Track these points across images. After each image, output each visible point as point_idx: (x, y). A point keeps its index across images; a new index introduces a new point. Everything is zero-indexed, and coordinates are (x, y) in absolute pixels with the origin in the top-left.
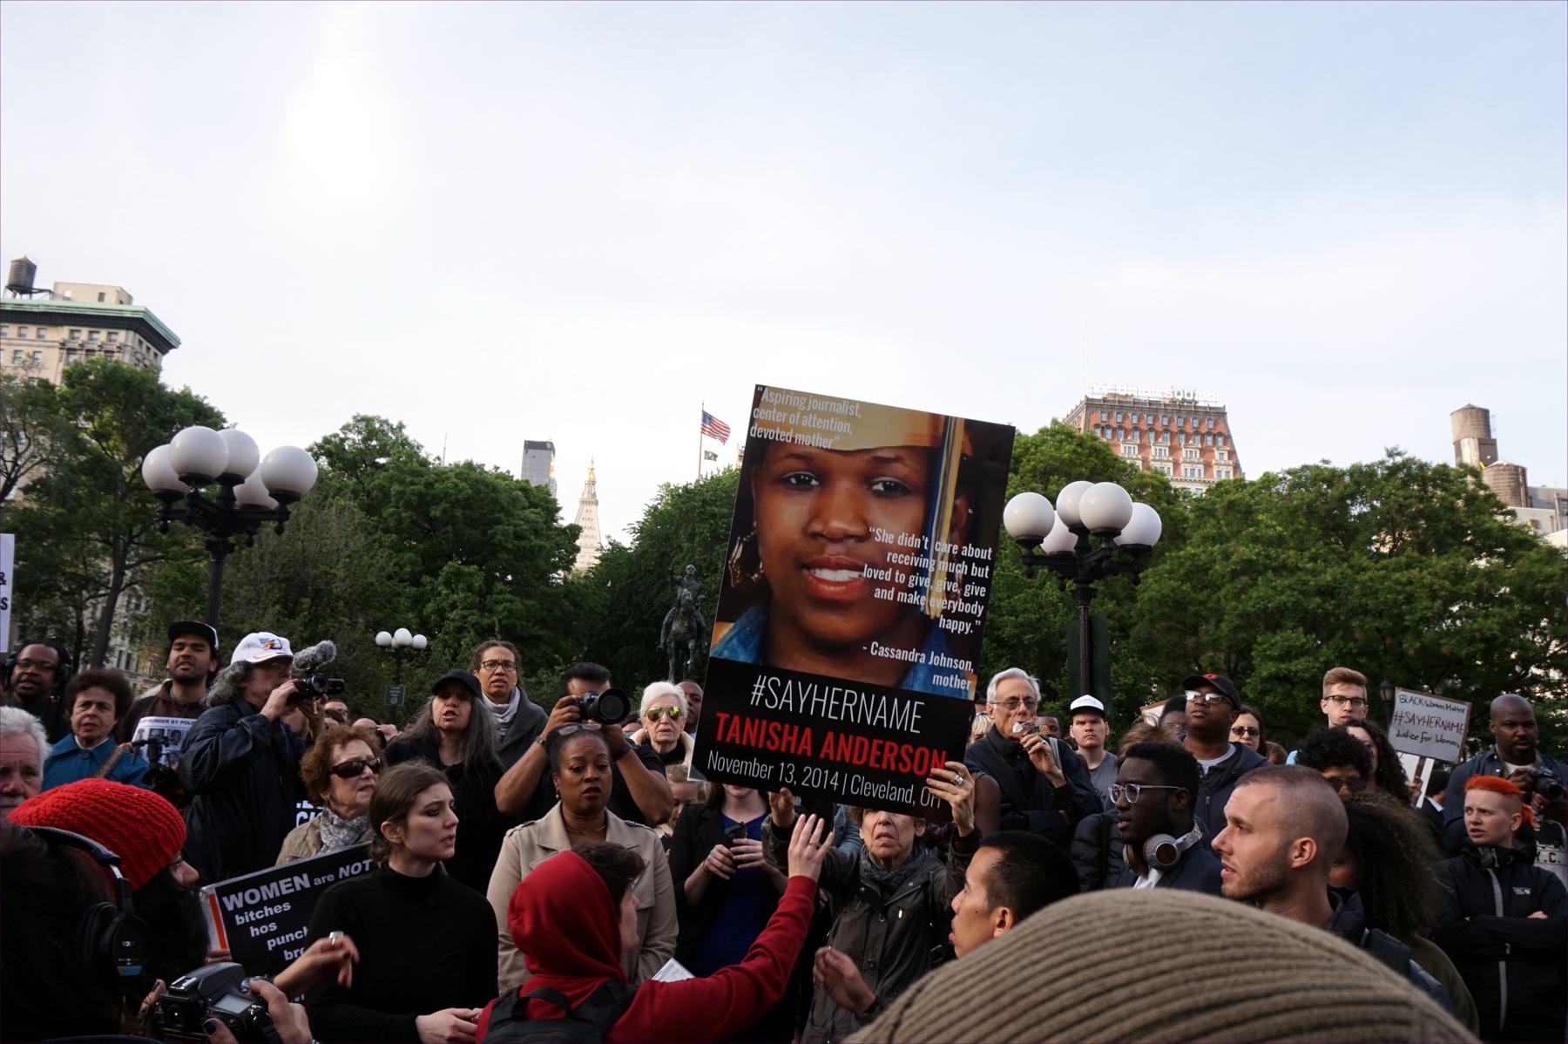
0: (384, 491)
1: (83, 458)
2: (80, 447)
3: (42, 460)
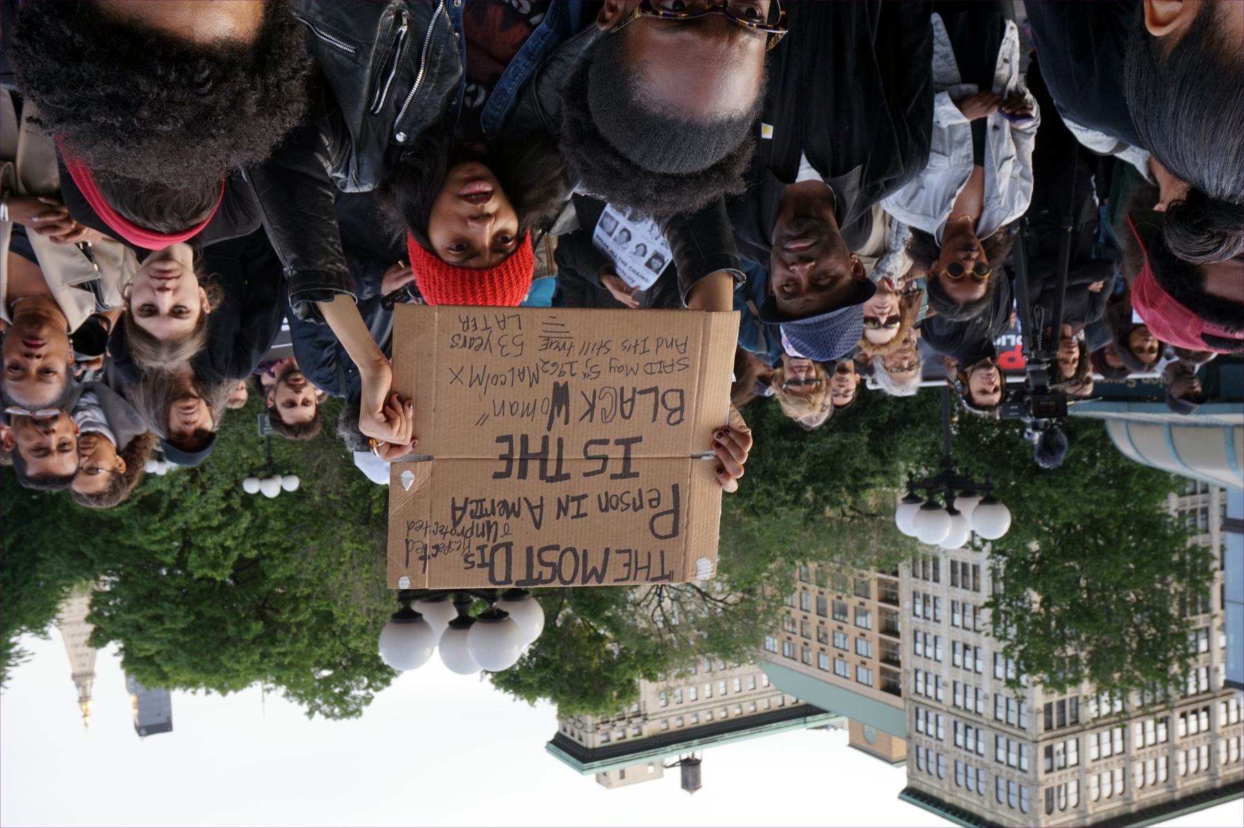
0: (316, 641)
3: (639, 604)
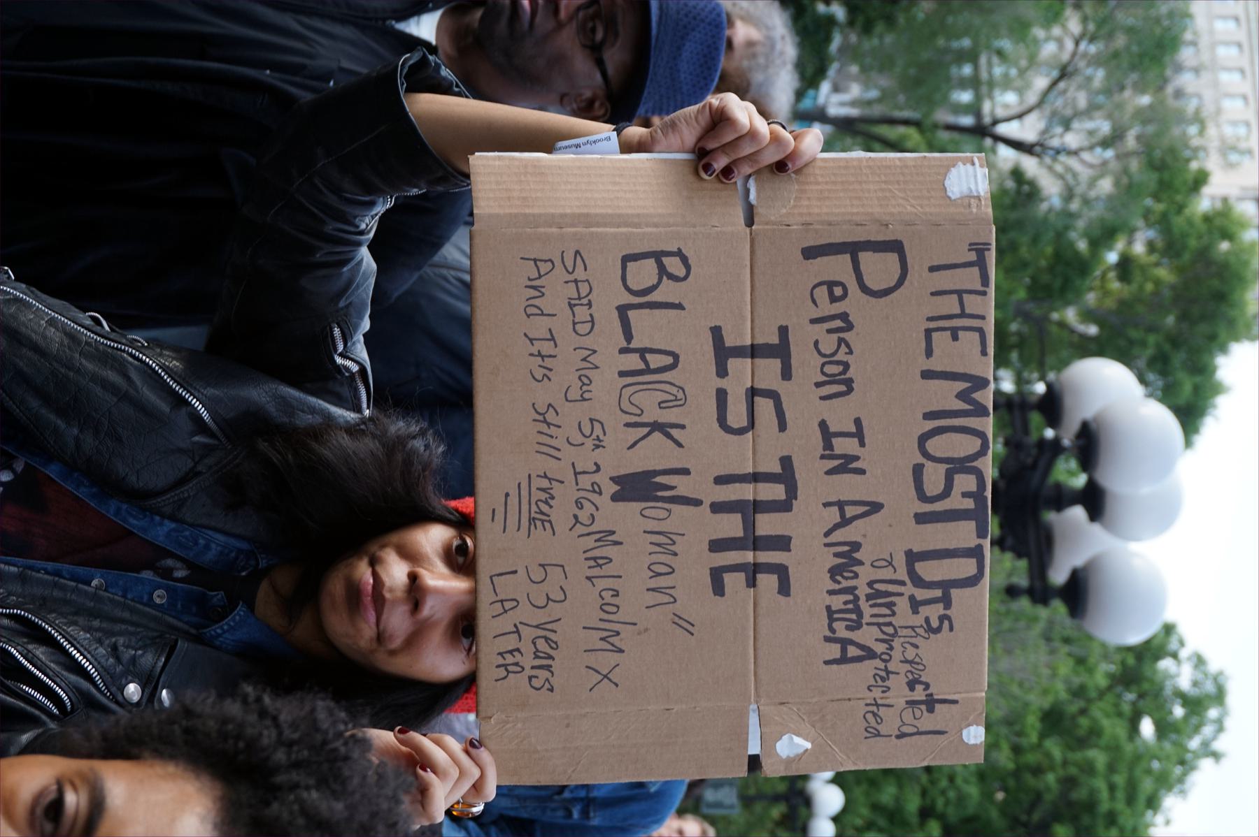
1: (1082, 245)
2: (1104, 235)
